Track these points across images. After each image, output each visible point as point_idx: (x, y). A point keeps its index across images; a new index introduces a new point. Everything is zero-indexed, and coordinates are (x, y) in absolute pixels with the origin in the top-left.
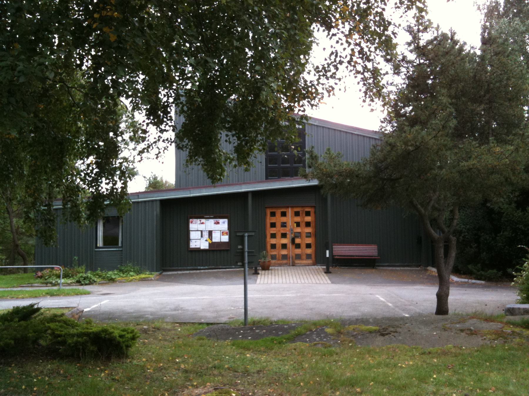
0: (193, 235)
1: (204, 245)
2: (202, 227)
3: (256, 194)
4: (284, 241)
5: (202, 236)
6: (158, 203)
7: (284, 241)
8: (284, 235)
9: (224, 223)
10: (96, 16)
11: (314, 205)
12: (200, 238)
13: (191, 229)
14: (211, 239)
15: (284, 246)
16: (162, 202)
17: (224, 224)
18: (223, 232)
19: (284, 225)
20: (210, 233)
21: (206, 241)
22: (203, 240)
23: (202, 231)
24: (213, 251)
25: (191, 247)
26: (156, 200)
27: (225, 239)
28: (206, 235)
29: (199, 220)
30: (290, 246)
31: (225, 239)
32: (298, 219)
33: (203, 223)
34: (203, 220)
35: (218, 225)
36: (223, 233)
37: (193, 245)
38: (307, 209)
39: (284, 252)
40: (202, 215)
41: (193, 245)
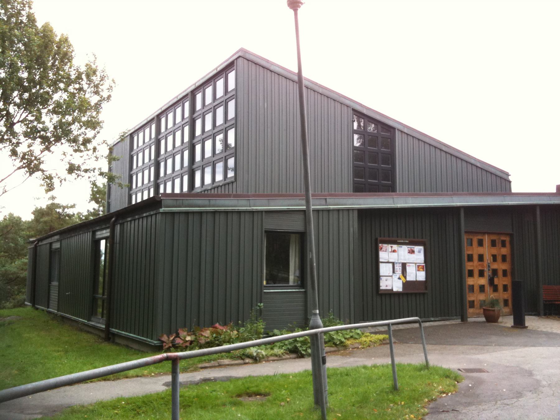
0: (385, 270)
1: (397, 286)
2: (393, 257)
3: (471, 211)
4: (483, 281)
5: (394, 272)
6: (356, 213)
7: (483, 281)
8: (481, 274)
9: (419, 252)
10: (13, 20)
11: (510, 232)
12: (391, 274)
13: (381, 260)
14: (405, 277)
15: (482, 288)
16: (363, 214)
17: (418, 255)
18: (418, 266)
19: (481, 258)
20: (404, 266)
21: (399, 278)
22: (395, 277)
23: (393, 264)
24: (407, 294)
25: (381, 288)
26: (353, 210)
27: (421, 276)
28: (398, 268)
29: (390, 245)
30: (488, 288)
31: (421, 276)
32: (494, 251)
33: (394, 251)
34: (395, 247)
35: (413, 255)
36: (419, 268)
37: (384, 285)
38: (503, 238)
39: (482, 297)
40: (394, 239)
41: (384, 285)
